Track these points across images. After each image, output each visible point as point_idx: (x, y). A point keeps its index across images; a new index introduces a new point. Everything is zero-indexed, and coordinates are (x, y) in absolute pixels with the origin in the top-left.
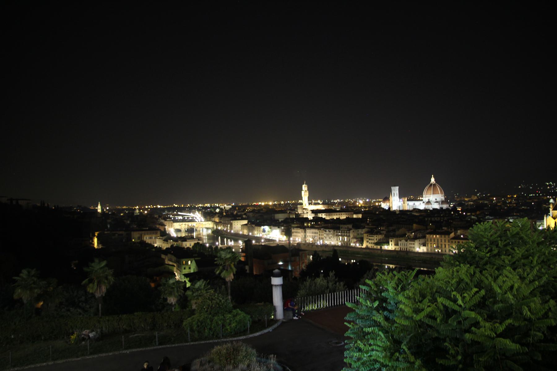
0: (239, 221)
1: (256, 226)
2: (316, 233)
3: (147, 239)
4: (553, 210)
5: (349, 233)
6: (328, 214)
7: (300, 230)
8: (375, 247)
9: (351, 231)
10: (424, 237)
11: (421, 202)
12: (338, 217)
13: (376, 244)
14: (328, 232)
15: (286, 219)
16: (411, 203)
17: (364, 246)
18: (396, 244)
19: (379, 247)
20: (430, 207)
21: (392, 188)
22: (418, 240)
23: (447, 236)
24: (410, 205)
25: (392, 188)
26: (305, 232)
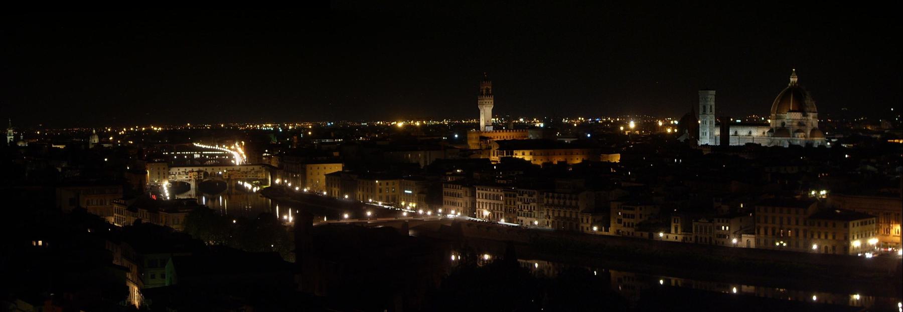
0: (322, 166)
3: (92, 204)
5: (577, 199)
6: (538, 152)
8: (638, 234)
11: (766, 130)
13: (641, 227)
14: (526, 196)
16: (743, 132)
17: (612, 231)
18: (687, 229)
19: (646, 235)
20: (784, 142)
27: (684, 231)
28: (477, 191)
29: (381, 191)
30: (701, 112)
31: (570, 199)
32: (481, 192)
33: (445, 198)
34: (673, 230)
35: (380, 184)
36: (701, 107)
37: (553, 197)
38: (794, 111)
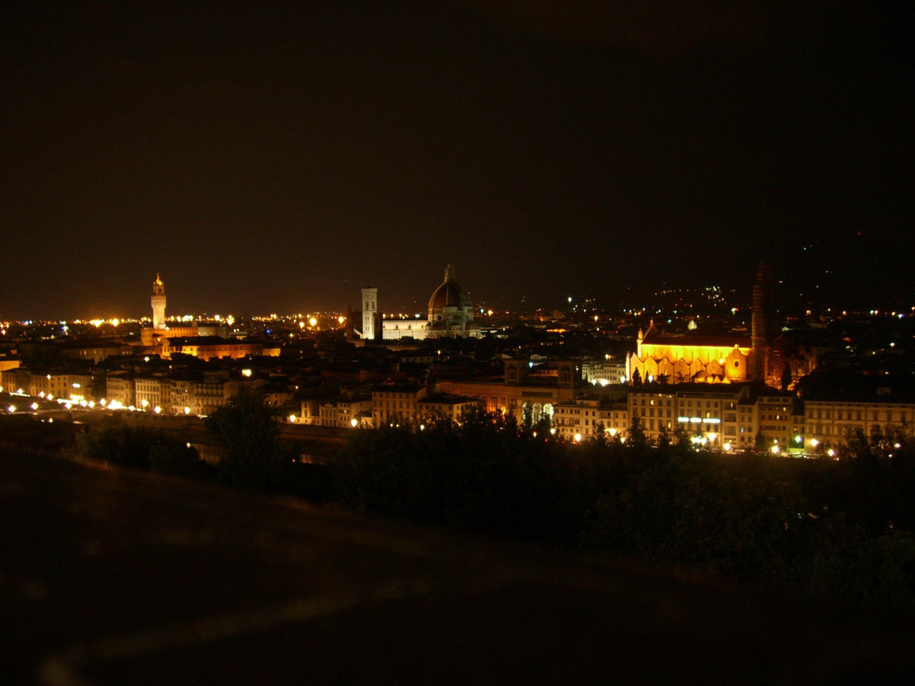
1: (34, 373)
2: (155, 389)
4: (643, 343)
5: (222, 389)
6: (205, 347)
7: (123, 383)
9: (226, 385)
10: (368, 398)
11: (425, 323)
12: (226, 354)
15: (111, 358)
16: (403, 326)
18: (315, 413)
21: (364, 291)
22: (359, 403)
23: (411, 395)
24: (393, 331)
25: (364, 291)
26: (133, 387)
27: (313, 414)
28: (137, 384)
29: (53, 385)
30: (364, 308)
31: (217, 388)
32: (140, 384)
33: (109, 391)
34: (303, 415)
35: (52, 379)
36: (364, 304)
37: (202, 387)
38: (449, 305)
